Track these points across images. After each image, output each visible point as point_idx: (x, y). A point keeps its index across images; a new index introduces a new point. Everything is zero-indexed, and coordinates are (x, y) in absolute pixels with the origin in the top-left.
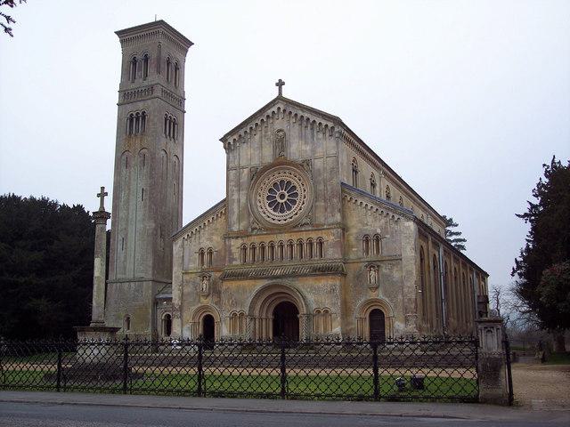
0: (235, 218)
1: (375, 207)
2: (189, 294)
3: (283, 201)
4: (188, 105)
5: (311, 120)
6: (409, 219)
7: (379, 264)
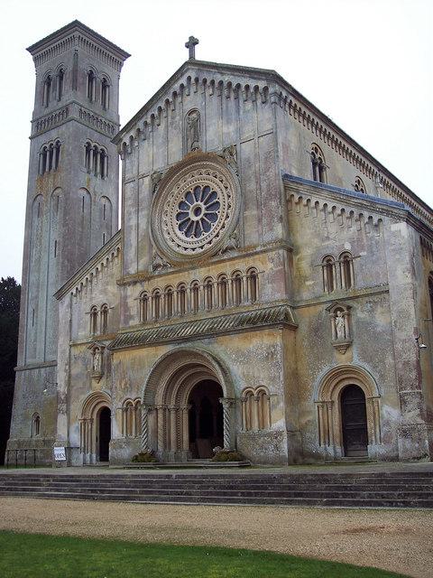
3: (202, 215)
5: (243, 85)
6: (398, 218)
7: (350, 303)
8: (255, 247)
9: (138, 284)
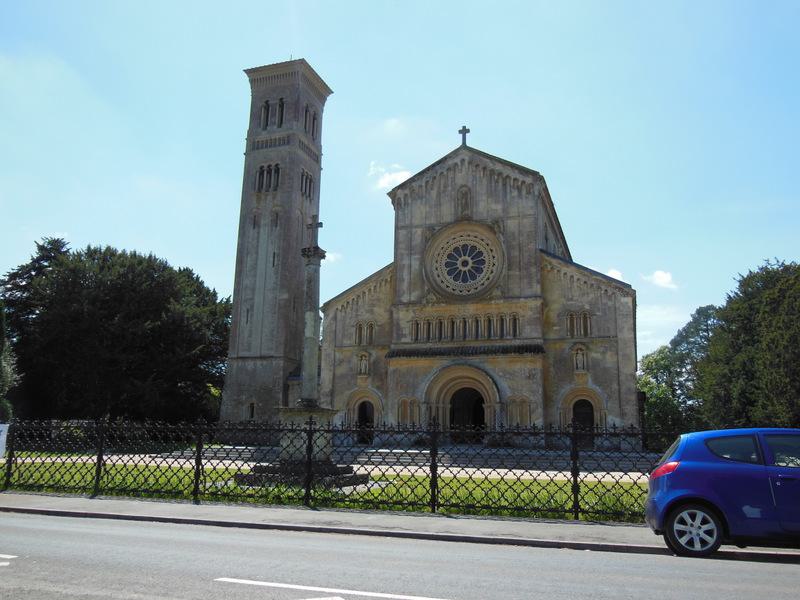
0: (405, 285)
2: (343, 376)
4: (325, 162)
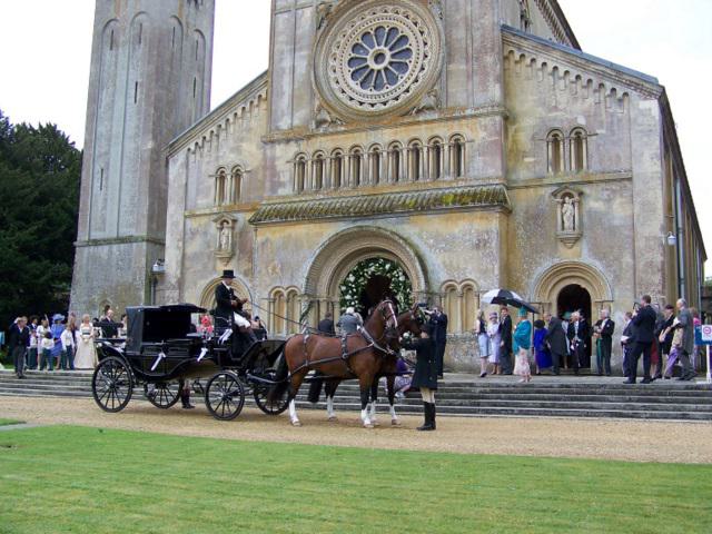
0: (285, 102)
1: (574, 72)
2: (196, 256)
3: (381, 67)
8: (464, 109)
9: (292, 143)
